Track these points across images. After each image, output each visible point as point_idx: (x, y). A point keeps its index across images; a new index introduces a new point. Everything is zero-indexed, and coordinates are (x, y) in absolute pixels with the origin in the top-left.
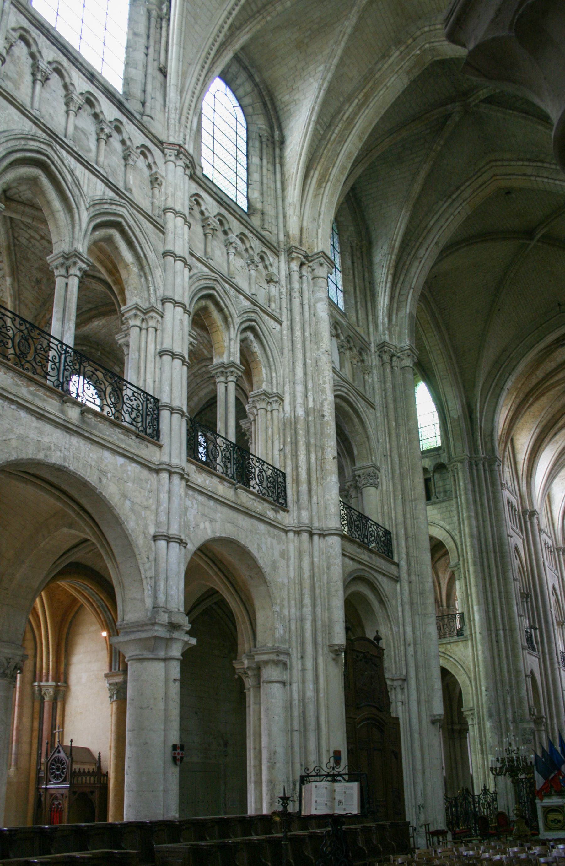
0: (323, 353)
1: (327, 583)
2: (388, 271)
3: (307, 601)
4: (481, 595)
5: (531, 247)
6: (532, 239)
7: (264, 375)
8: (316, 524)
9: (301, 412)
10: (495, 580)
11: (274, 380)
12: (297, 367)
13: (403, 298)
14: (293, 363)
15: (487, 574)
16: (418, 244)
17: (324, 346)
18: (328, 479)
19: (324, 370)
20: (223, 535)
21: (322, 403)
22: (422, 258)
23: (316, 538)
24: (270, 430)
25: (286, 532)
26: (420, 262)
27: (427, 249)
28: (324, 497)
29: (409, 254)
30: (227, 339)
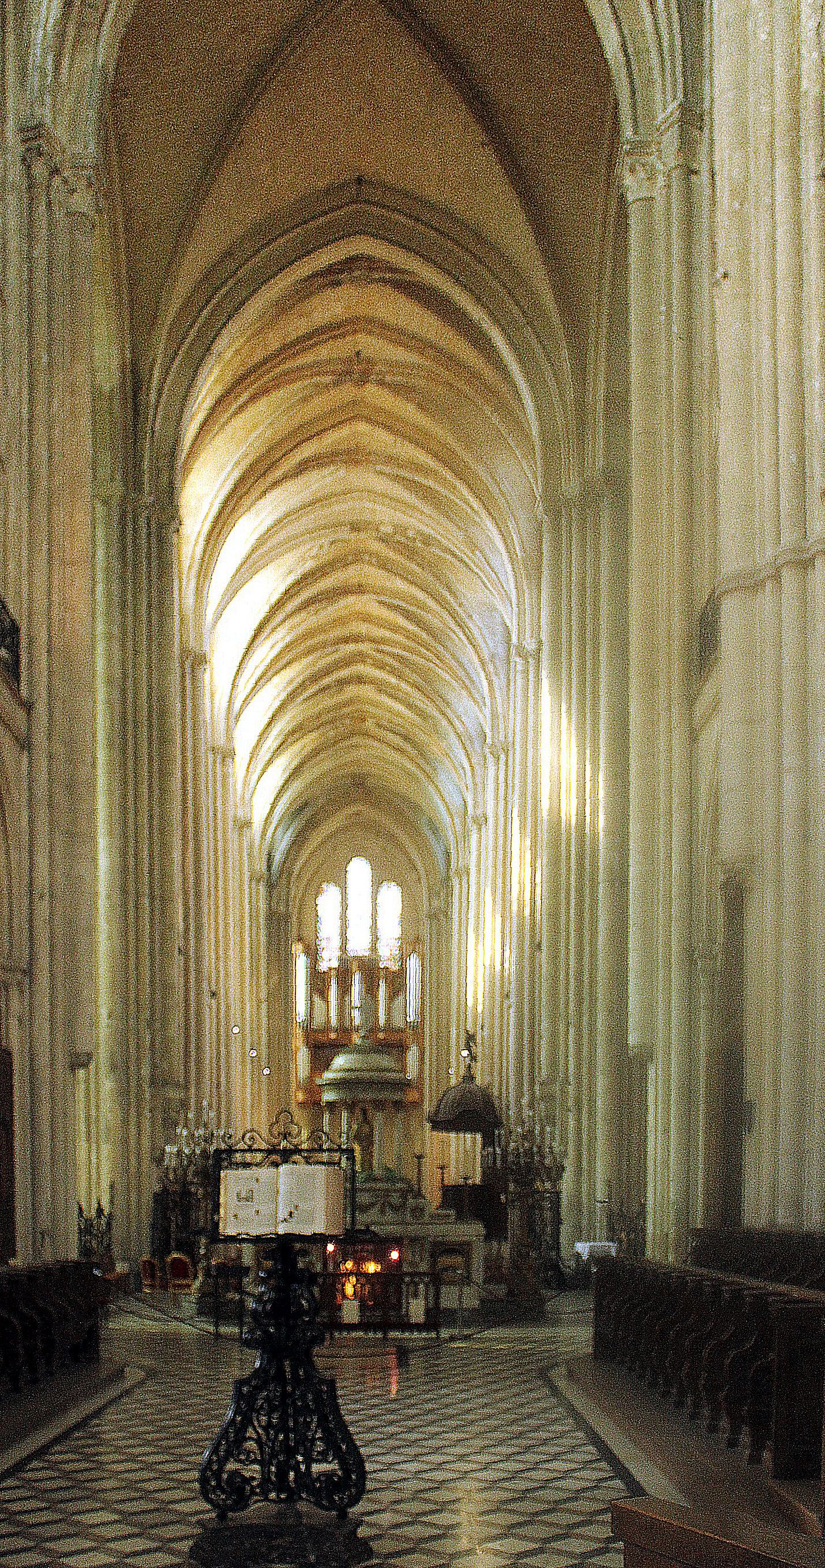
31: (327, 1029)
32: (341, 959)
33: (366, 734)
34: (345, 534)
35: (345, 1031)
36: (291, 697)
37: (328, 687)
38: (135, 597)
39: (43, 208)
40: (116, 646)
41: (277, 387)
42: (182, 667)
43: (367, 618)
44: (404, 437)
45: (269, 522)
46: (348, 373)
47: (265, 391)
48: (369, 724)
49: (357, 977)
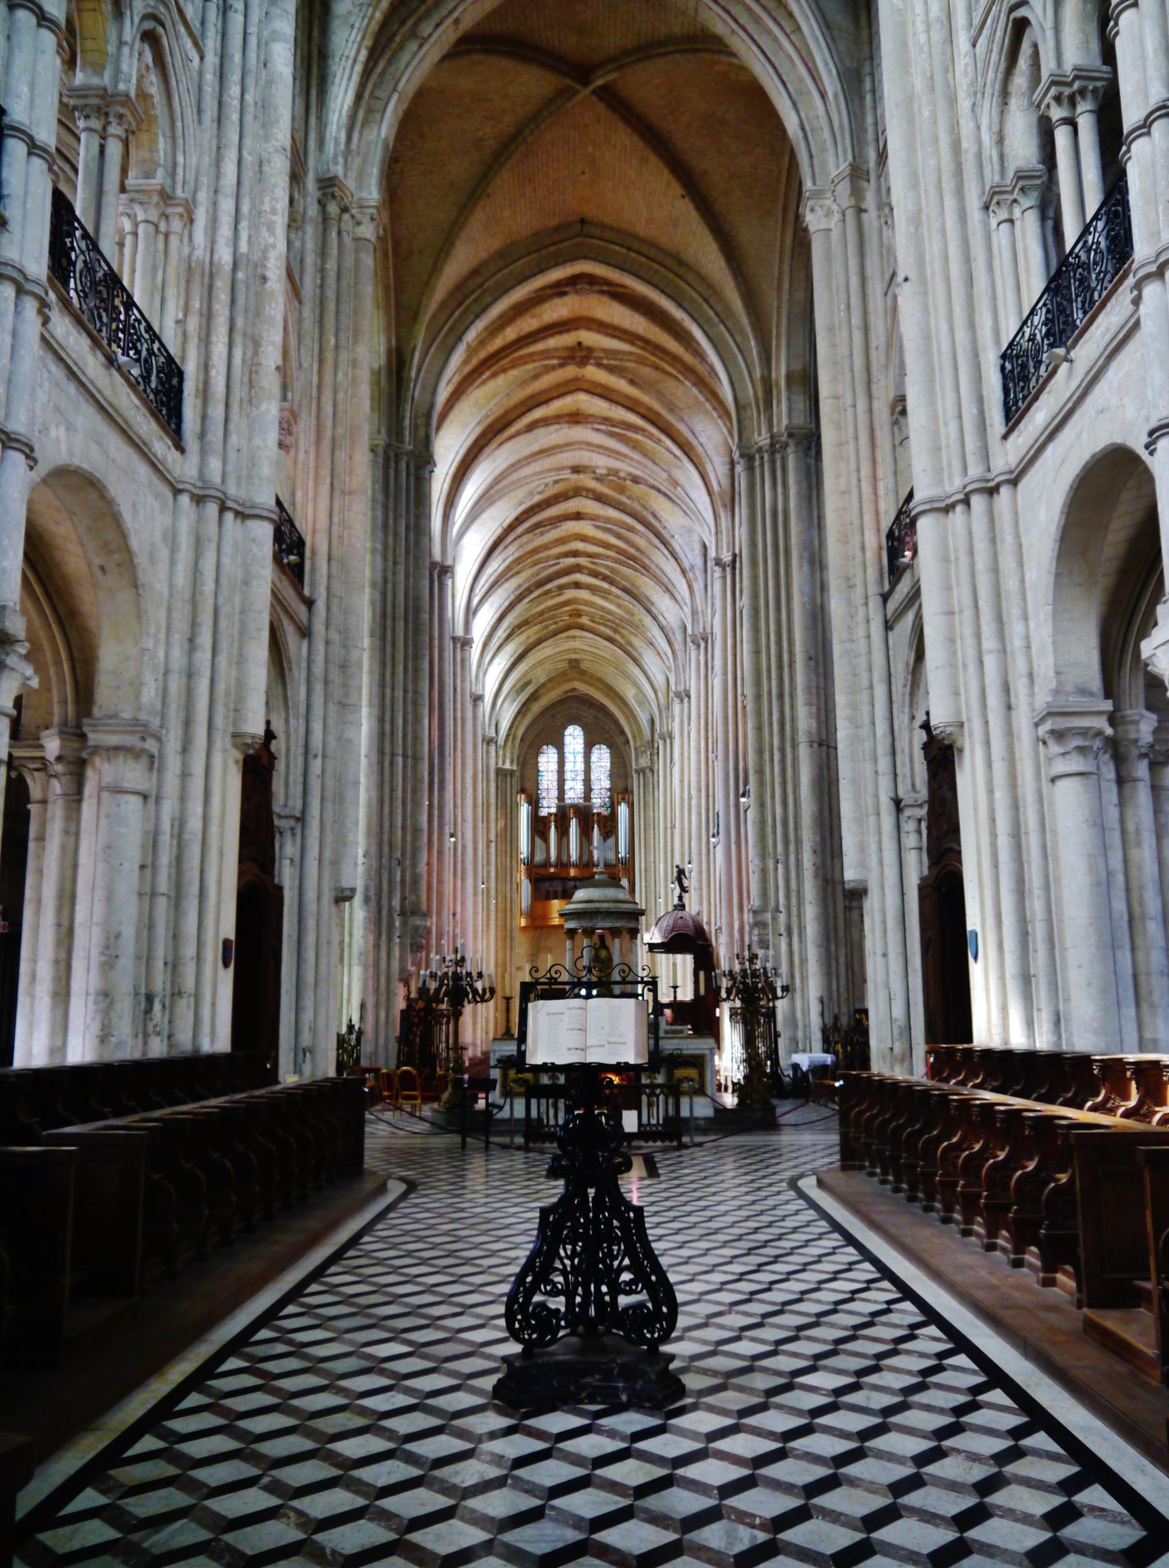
0: (277, 151)
1: (242, 612)
2: (363, 38)
3: (205, 638)
4: (376, 689)
5: (579, 97)
6: (586, 84)
7: (162, 153)
8: (232, 490)
9: (225, 255)
10: (400, 669)
11: (180, 170)
12: (227, 160)
13: (379, 105)
14: (219, 148)
15: (389, 656)
16: (423, 8)
17: (280, 136)
18: (263, 407)
19: (275, 186)
20: (85, 466)
21: (265, 252)
22: (425, 40)
23: (229, 516)
24: (160, 273)
25: (177, 492)
26: (421, 46)
27: (438, 25)
28: (250, 440)
29: (403, 22)
30: (113, 37)
31: (547, 864)
32: (558, 807)
33: (582, 627)
34: (566, 474)
35: (563, 865)
36: (519, 599)
37: (549, 591)
38: (395, 519)
39: (334, 235)
40: (379, 558)
41: (512, 367)
42: (431, 575)
43: (584, 538)
44: (617, 403)
45: (504, 466)
46: (572, 358)
47: (504, 370)
48: (584, 620)
49: (574, 823)
